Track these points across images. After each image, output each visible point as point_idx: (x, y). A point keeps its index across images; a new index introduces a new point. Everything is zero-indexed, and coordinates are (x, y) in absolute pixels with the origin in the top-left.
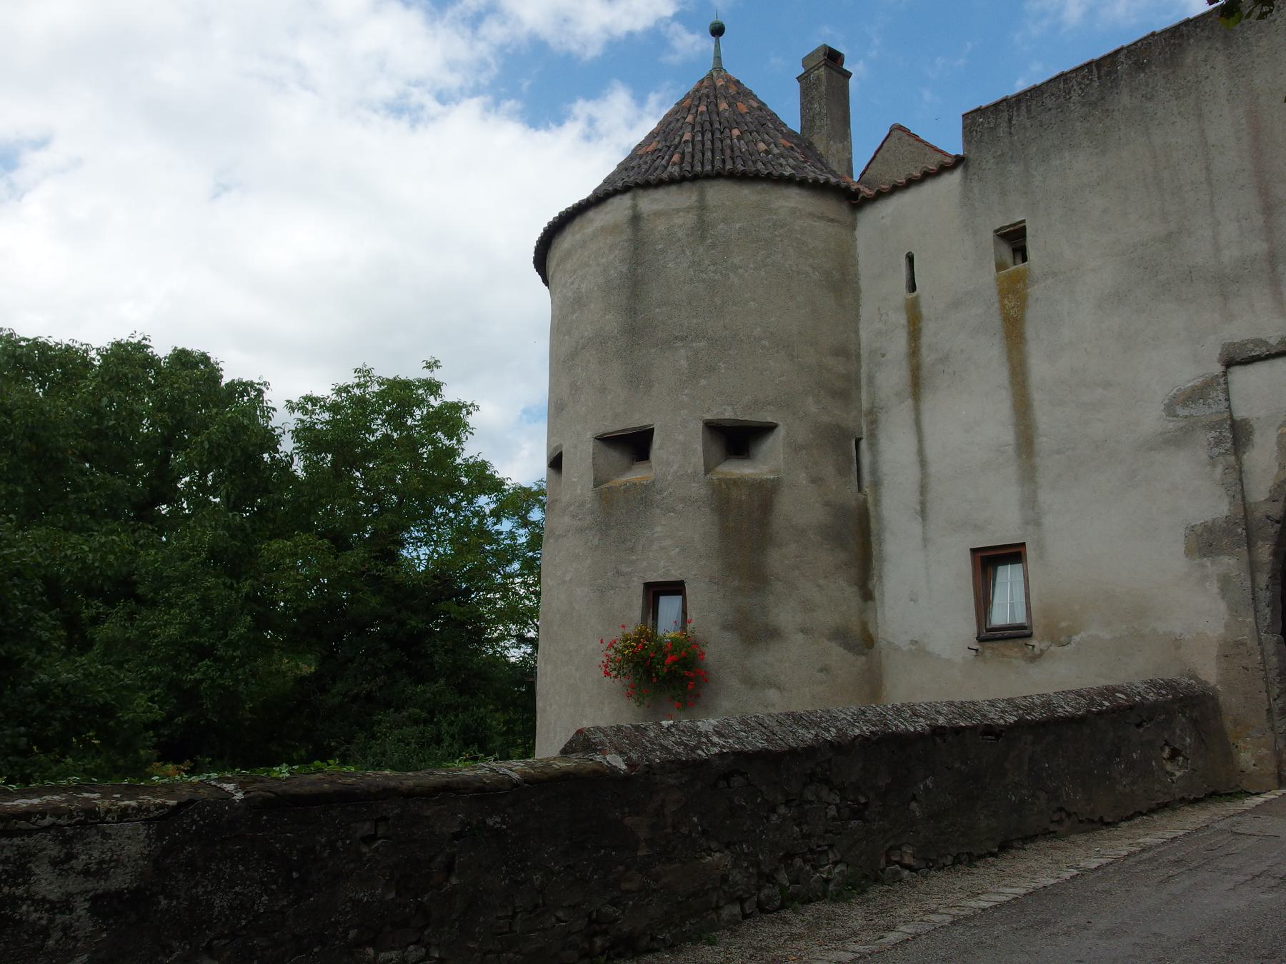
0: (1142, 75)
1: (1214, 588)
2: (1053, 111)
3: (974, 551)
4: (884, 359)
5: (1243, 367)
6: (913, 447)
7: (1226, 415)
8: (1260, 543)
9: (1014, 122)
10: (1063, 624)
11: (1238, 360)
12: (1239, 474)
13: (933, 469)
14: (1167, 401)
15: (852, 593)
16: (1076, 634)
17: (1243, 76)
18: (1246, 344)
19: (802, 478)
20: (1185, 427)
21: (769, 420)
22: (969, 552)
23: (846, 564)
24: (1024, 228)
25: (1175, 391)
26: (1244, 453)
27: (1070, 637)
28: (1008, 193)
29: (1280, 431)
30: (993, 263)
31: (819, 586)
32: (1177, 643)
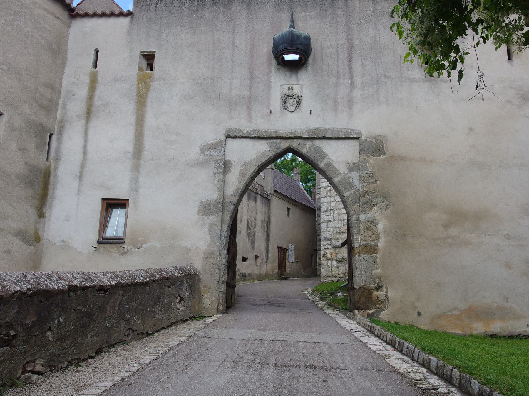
0: (215, 7)
1: (206, 229)
2: (176, 8)
3: (103, 200)
4: (74, 97)
5: (232, 139)
6: (81, 143)
7: (223, 157)
8: (226, 212)
9: (158, 6)
10: (140, 239)
11: (231, 136)
12: (223, 182)
13: (89, 157)
14: (201, 147)
15: (32, 213)
16: (145, 244)
17: (252, 23)
18: (235, 130)
19: (14, 146)
20: (206, 159)
22: (100, 200)
23: (32, 197)
24: (154, 55)
25: (205, 143)
26: (227, 174)
27: (142, 245)
28: (150, 37)
29: (241, 168)
30: (137, 66)
31: (12, 206)
32: (188, 251)
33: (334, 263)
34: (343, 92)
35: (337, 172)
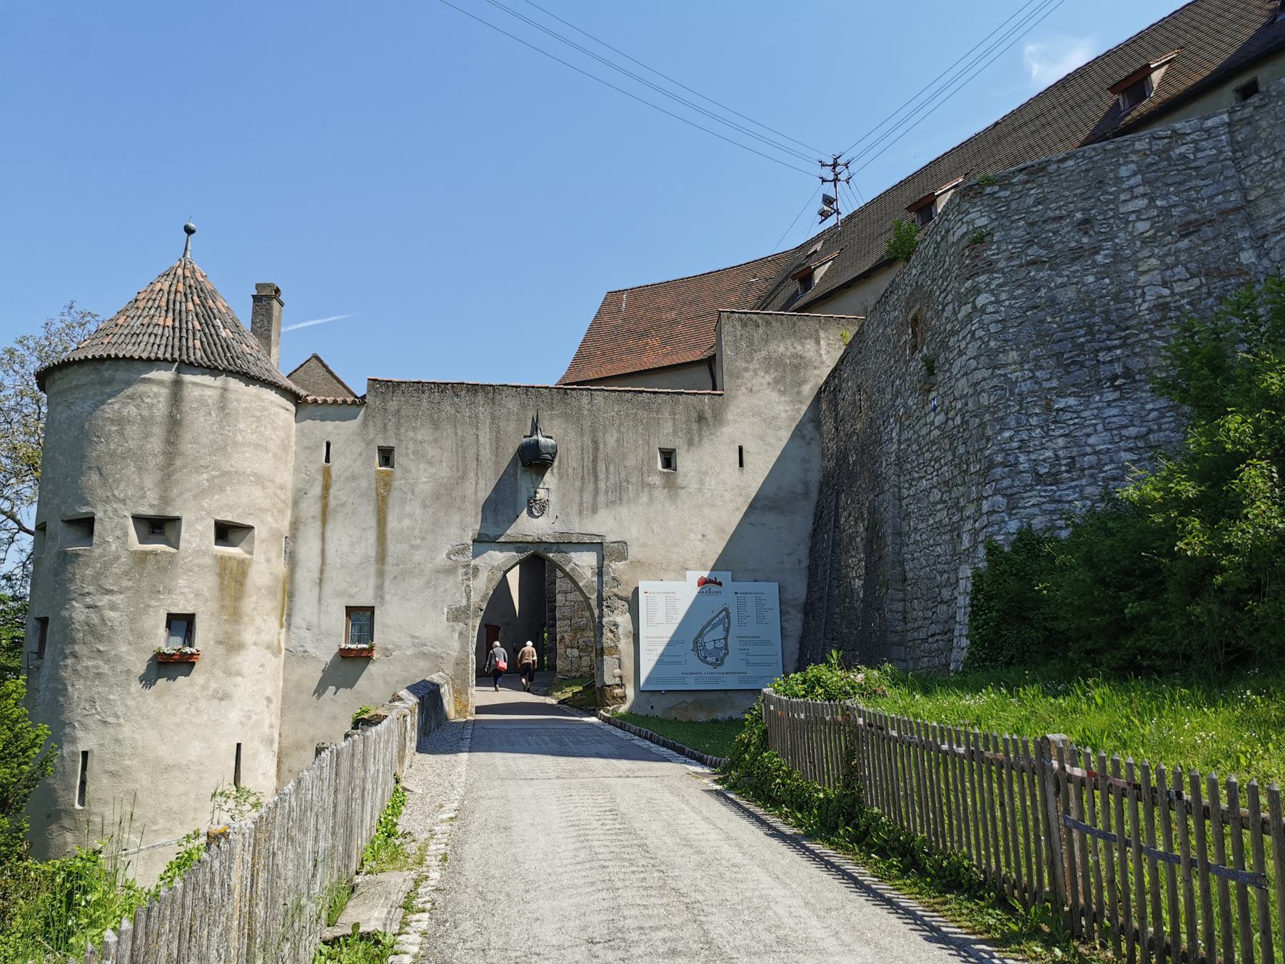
21: (250, 524)
33: (576, 652)
34: (587, 497)
35: (581, 576)
